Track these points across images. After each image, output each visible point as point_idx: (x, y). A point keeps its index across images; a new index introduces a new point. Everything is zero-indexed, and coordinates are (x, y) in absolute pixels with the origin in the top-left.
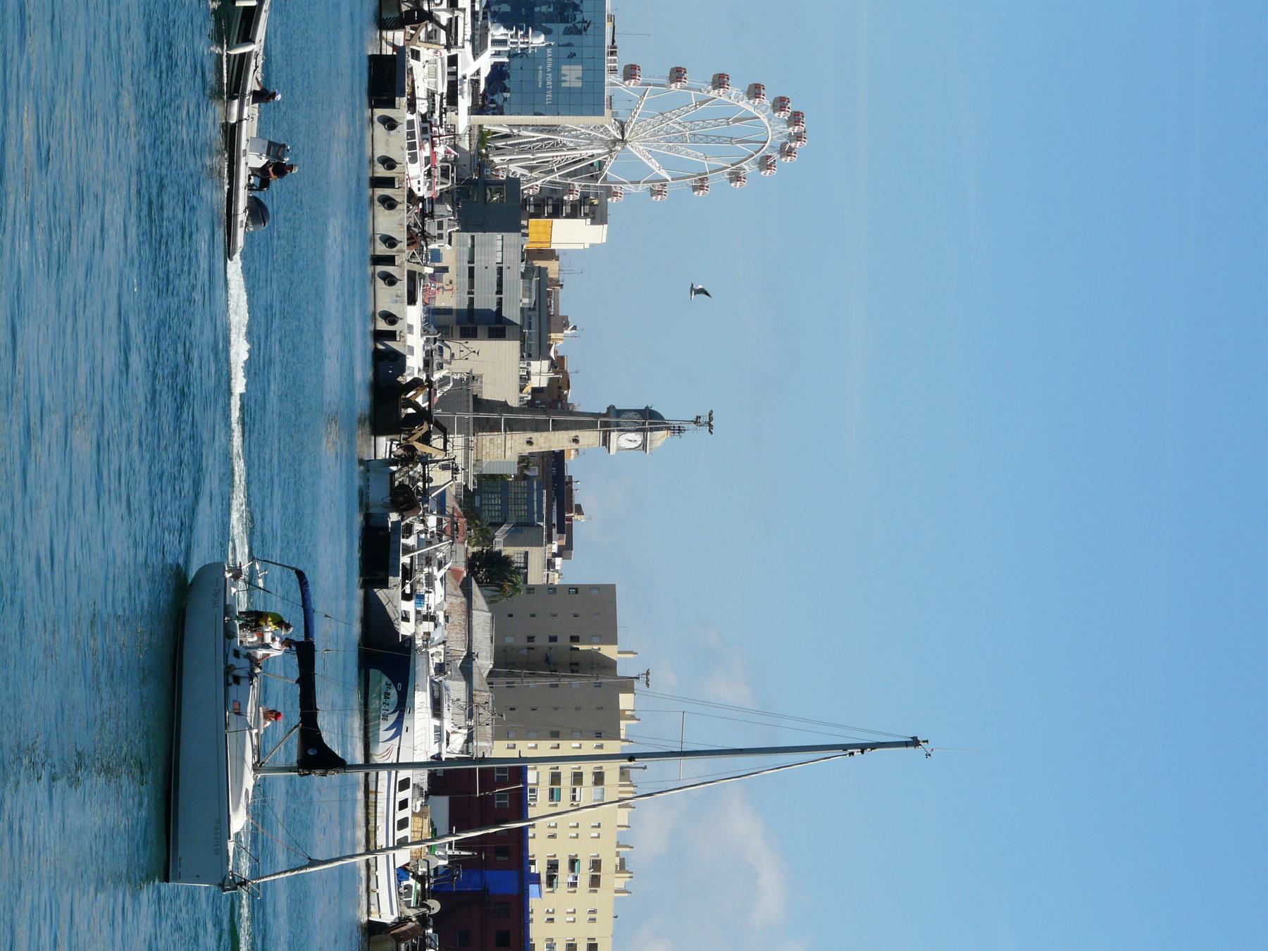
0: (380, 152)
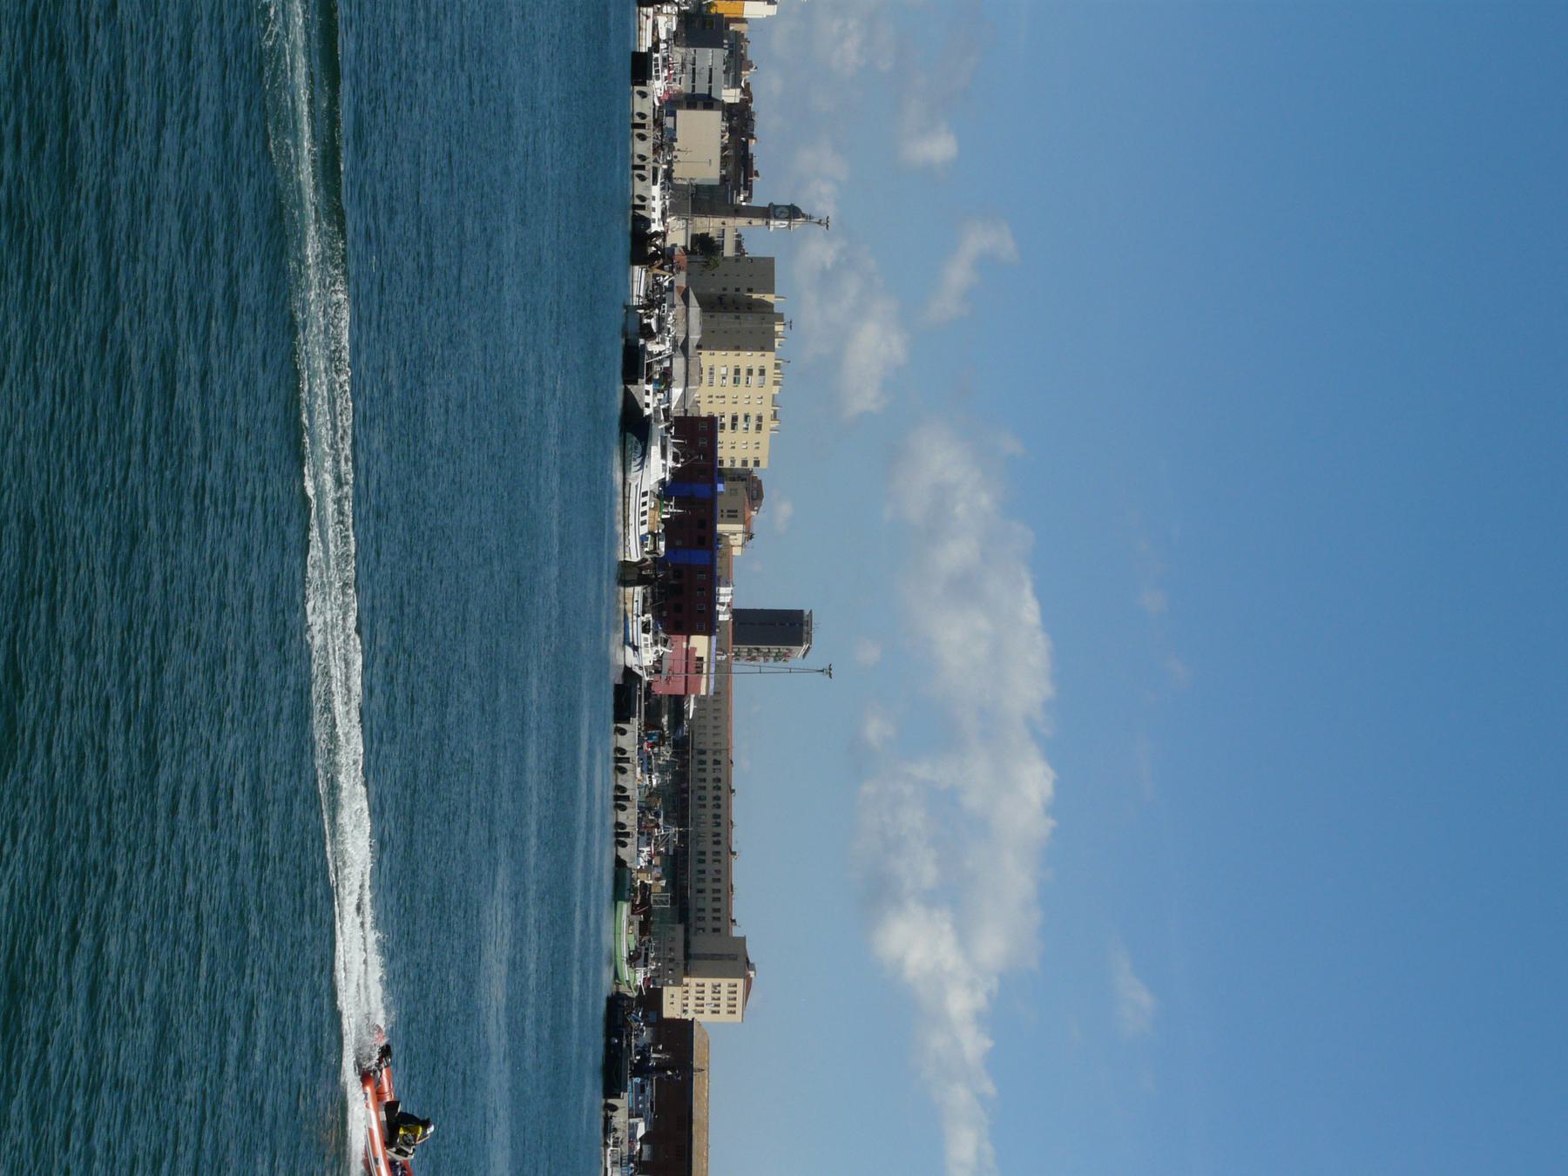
0: (637, 109)
